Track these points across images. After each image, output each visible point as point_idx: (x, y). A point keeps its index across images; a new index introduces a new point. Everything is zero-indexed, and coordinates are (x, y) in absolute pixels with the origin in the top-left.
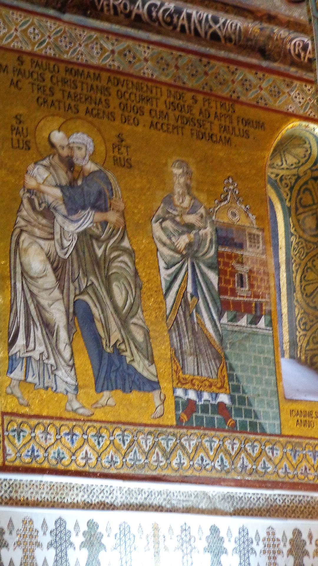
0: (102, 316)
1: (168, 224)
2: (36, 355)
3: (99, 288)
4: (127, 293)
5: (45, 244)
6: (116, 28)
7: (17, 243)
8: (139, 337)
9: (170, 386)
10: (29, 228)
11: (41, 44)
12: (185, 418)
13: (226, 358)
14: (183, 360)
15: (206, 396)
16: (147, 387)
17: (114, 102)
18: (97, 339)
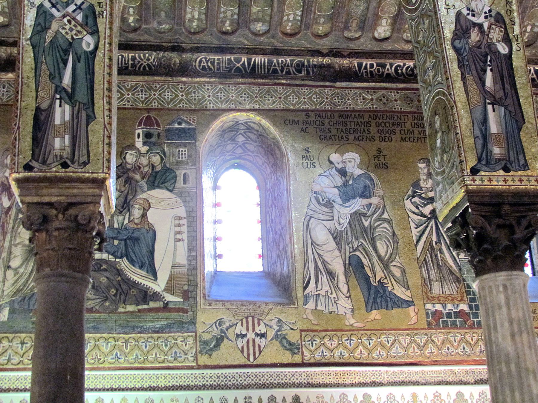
0: (369, 263)
1: (416, 199)
2: (323, 293)
3: (367, 246)
4: (388, 247)
5: (328, 224)
6: (372, 84)
7: (308, 225)
8: (397, 273)
9: (422, 302)
10: (316, 215)
11: (321, 104)
12: (434, 323)
13: (464, 280)
14: (431, 285)
15: (449, 307)
16: (405, 305)
17: (374, 130)
18: (367, 279)
